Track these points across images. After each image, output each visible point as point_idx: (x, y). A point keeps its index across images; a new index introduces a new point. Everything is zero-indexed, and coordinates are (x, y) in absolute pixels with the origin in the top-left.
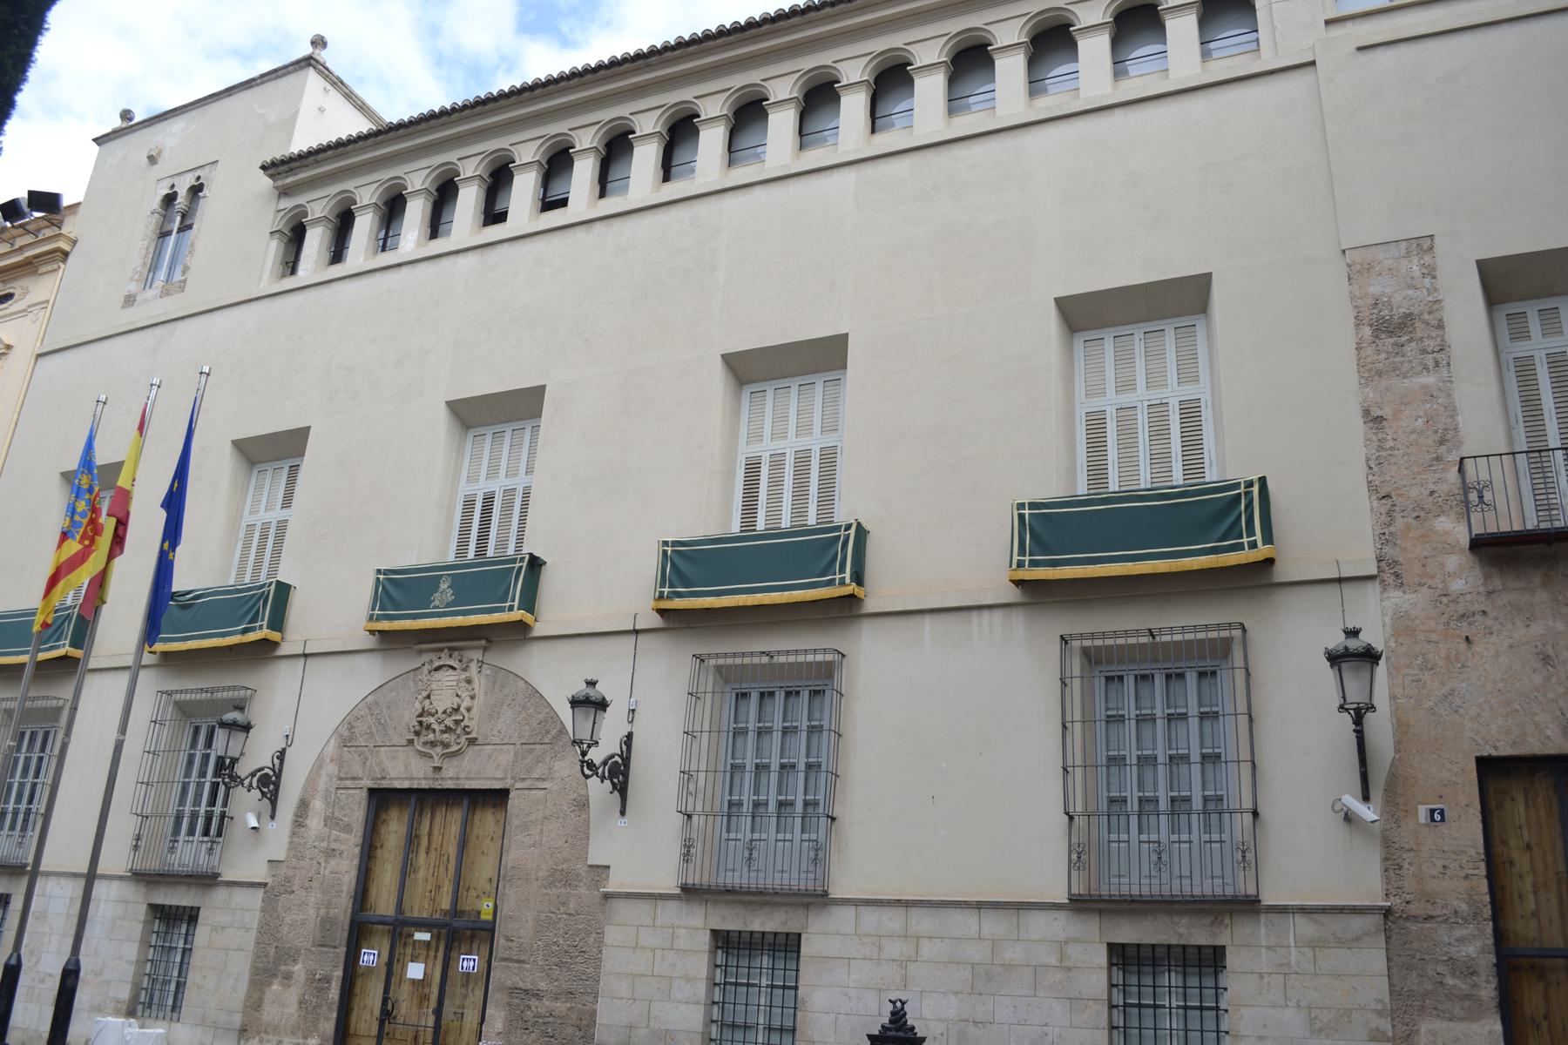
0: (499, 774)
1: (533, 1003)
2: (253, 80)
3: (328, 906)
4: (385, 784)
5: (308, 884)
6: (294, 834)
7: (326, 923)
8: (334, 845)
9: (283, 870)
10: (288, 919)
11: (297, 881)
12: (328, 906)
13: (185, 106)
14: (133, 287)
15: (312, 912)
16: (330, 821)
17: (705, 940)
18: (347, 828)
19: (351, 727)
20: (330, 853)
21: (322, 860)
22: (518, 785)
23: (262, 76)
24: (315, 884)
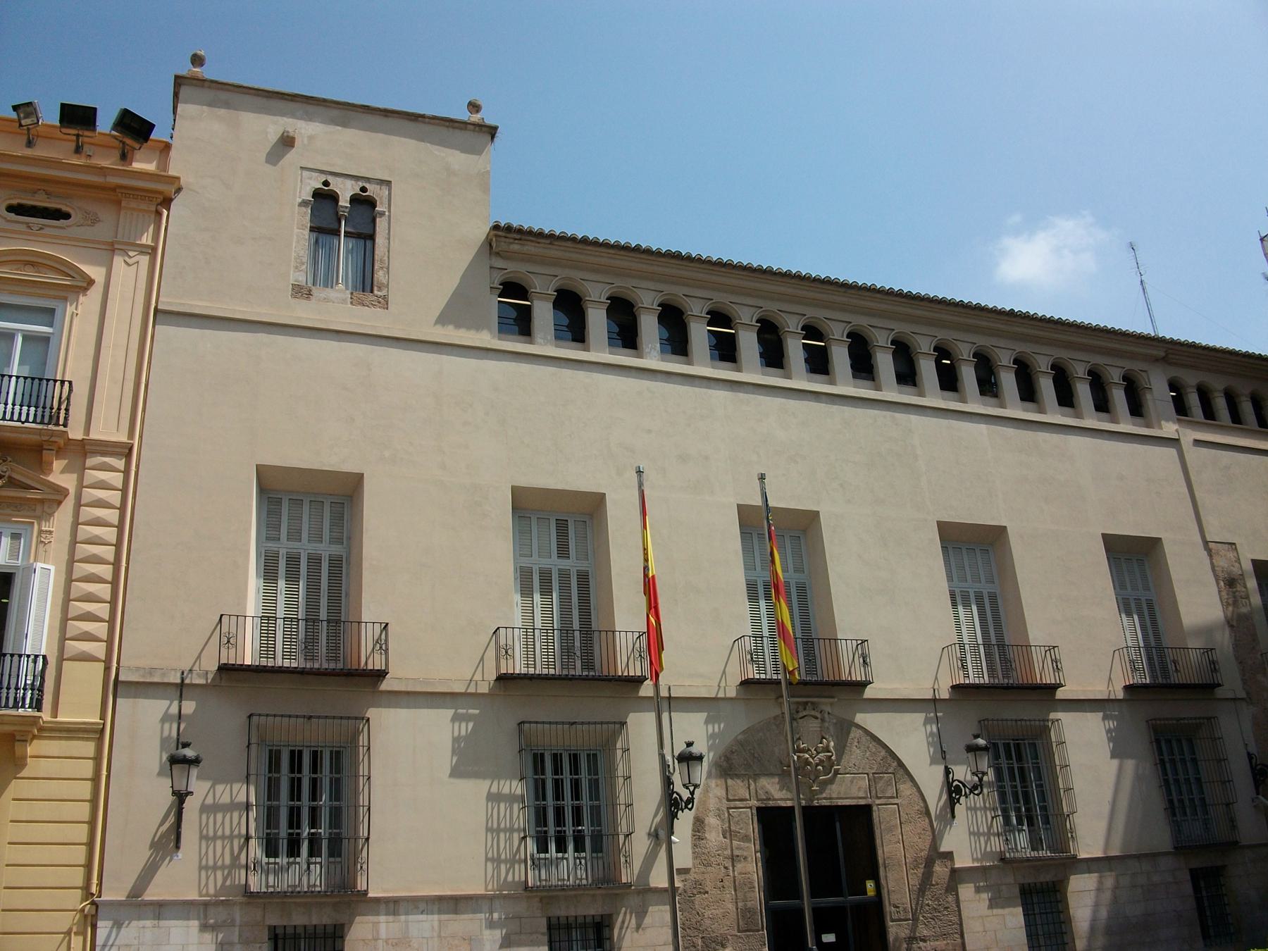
0: (861, 794)
1: (921, 944)
2: (423, 116)
3: (745, 900)
4: (771, 804)
5: (720, 884)
6: (695, 845)
7: (745, 914)
8: (736, 852)
9: (691, 876)
10: (708, 913)
11: (708, 883)
12: (745, 900)
13: (325, 100)
14: (301, 278)
15: (731, 906)
16: (728, 833)
17: (1017, 891)
18: (746, 838)
19: (727, 759)
20: (733, 859)
21: (729, 864)
22: (878, 802)
23: (434, 118)
24: (726, 883)
